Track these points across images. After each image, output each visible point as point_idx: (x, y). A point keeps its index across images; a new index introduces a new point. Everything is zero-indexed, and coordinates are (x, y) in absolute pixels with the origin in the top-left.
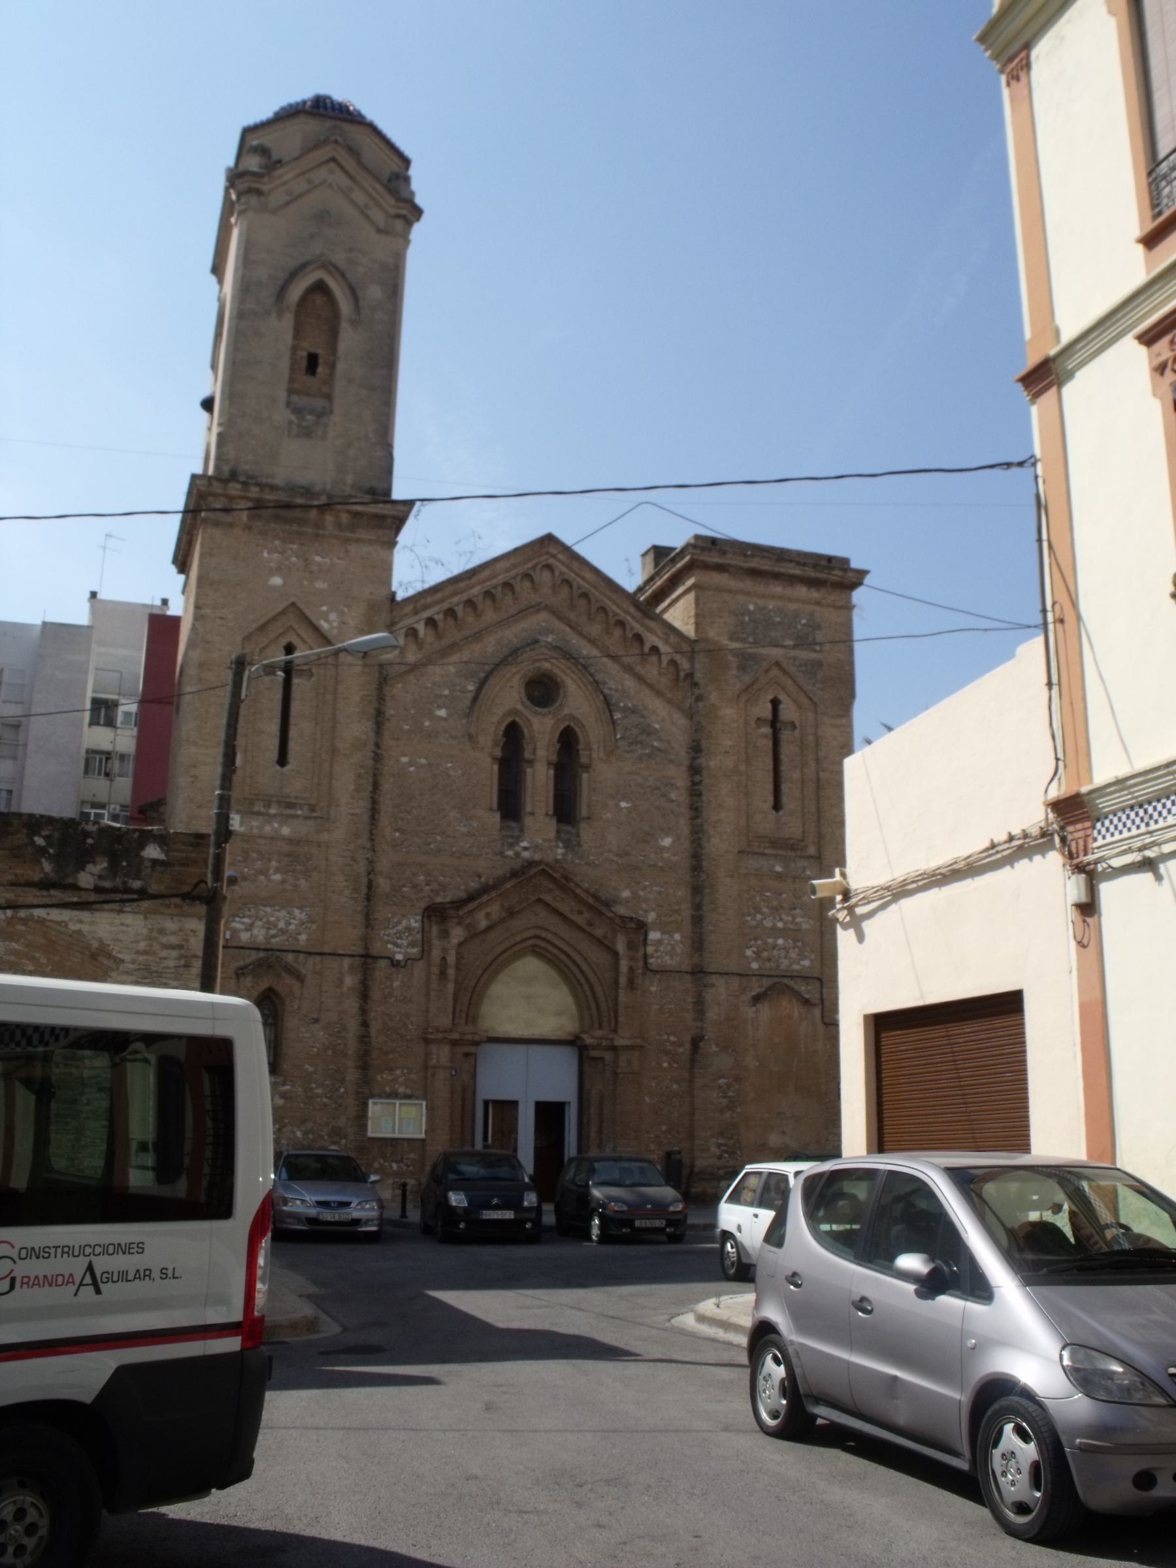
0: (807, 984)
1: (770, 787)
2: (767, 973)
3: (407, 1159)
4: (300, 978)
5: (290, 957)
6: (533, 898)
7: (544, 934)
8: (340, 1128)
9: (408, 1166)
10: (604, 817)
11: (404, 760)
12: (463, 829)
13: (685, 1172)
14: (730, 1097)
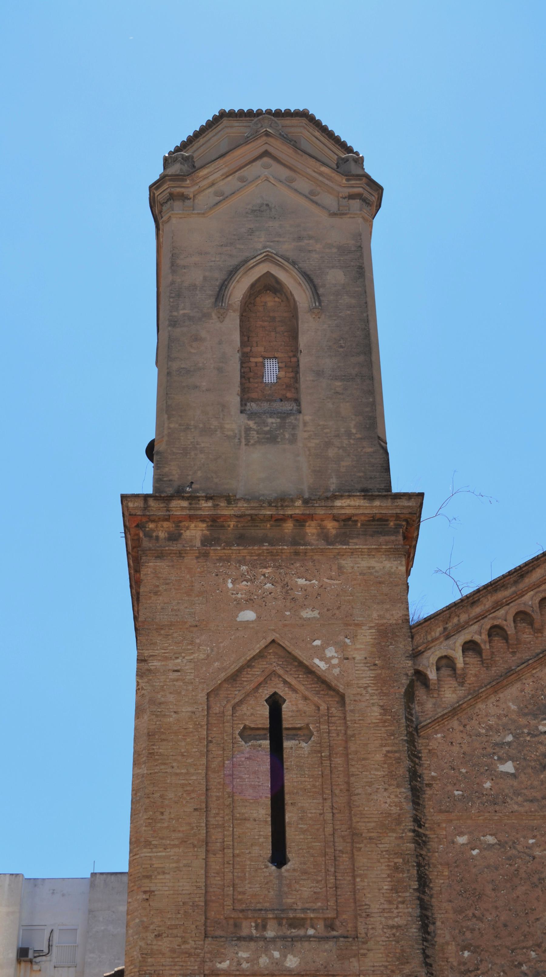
11: (462, 840)
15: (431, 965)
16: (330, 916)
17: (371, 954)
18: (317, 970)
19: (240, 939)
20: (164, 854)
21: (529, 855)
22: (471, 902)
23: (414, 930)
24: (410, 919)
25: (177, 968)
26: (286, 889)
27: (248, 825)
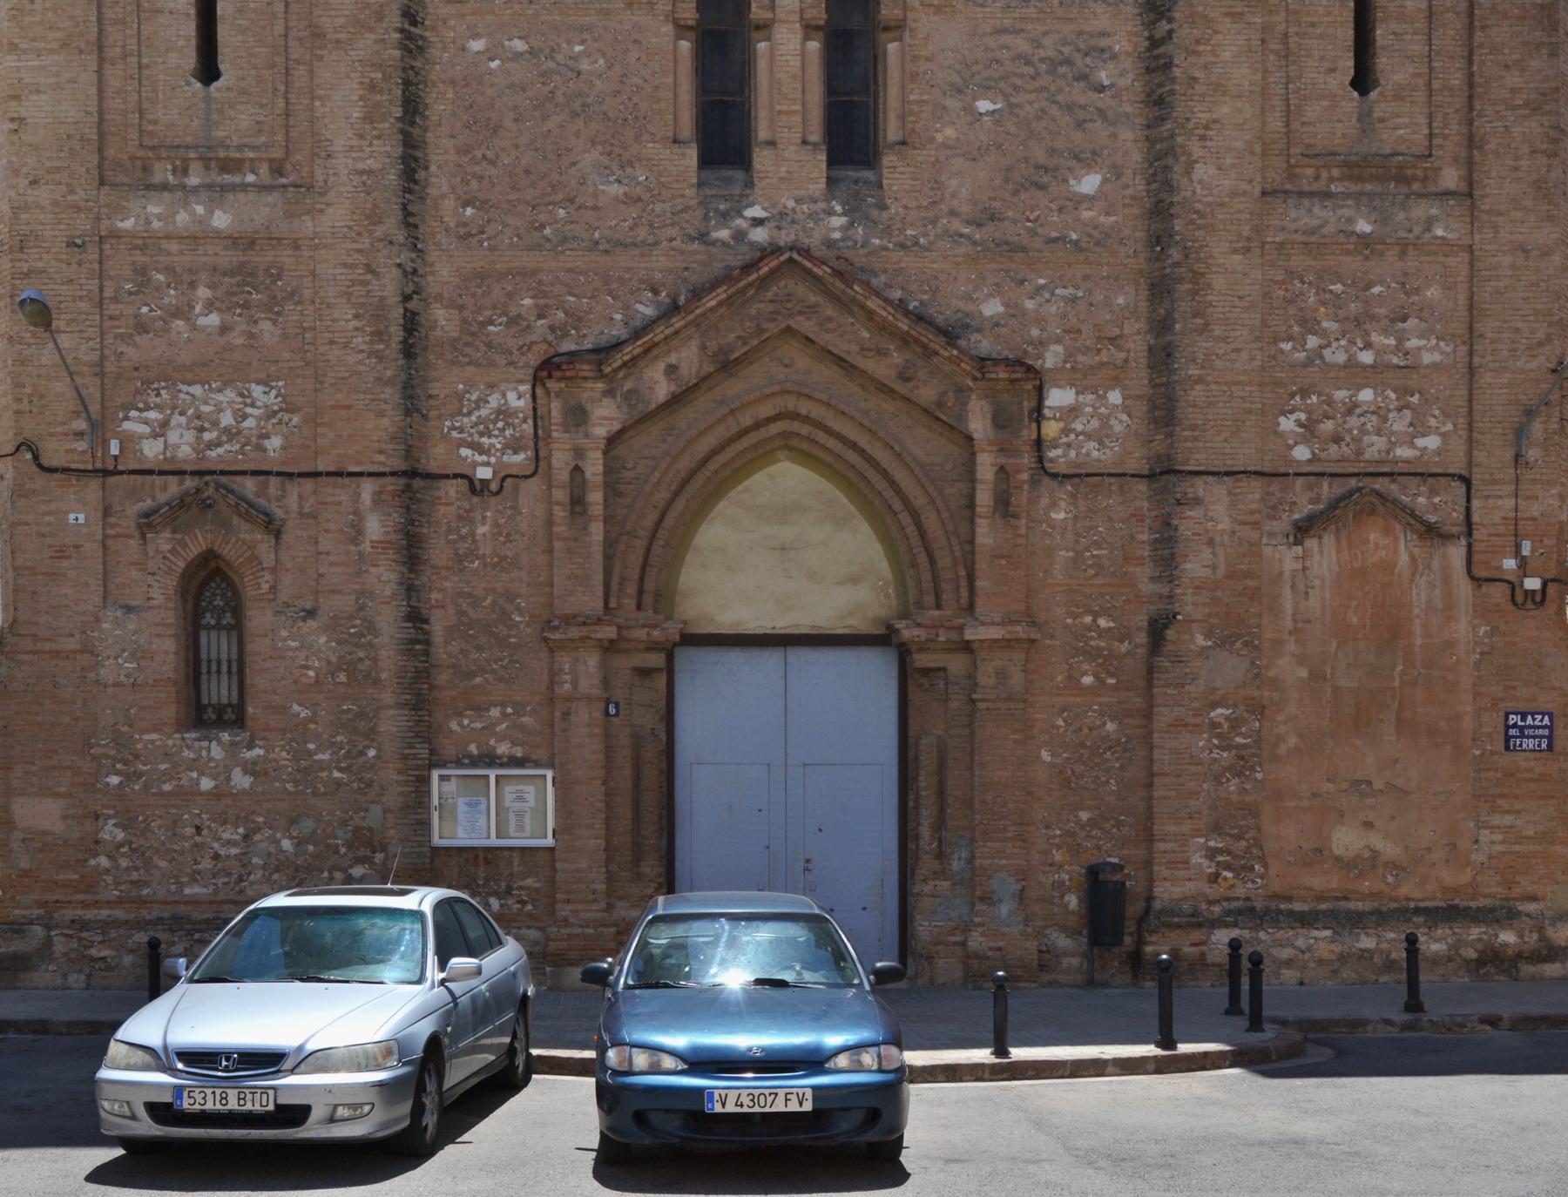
0: (1433, 492)
1: (1349, 33)
2: (1328, 470)
3: (521, 888)
4: (272, 527)
5: (249, 486)
6: (772, 328)
7: (804, 407)
8: (370, 829)
9: (523, 903)
10: (939, 138)
11: (477, 45)
12: (615, 190)
13: (1133, 909)
14: (1245, 746)
15: (416, 227)
16: (276, 156)
17: (330, 210)
18: (256, 232)
19: (150, 187)
20: (37, 63)
21: (572, 70)
22: (481, 137)
23: (392, 177)
24: (387, 160)
25: (61, 227)
26: (215, 116)
27: (162, 20)
